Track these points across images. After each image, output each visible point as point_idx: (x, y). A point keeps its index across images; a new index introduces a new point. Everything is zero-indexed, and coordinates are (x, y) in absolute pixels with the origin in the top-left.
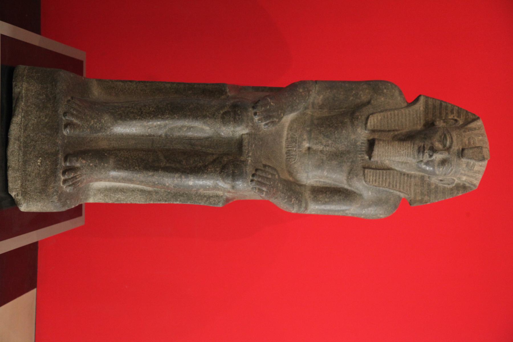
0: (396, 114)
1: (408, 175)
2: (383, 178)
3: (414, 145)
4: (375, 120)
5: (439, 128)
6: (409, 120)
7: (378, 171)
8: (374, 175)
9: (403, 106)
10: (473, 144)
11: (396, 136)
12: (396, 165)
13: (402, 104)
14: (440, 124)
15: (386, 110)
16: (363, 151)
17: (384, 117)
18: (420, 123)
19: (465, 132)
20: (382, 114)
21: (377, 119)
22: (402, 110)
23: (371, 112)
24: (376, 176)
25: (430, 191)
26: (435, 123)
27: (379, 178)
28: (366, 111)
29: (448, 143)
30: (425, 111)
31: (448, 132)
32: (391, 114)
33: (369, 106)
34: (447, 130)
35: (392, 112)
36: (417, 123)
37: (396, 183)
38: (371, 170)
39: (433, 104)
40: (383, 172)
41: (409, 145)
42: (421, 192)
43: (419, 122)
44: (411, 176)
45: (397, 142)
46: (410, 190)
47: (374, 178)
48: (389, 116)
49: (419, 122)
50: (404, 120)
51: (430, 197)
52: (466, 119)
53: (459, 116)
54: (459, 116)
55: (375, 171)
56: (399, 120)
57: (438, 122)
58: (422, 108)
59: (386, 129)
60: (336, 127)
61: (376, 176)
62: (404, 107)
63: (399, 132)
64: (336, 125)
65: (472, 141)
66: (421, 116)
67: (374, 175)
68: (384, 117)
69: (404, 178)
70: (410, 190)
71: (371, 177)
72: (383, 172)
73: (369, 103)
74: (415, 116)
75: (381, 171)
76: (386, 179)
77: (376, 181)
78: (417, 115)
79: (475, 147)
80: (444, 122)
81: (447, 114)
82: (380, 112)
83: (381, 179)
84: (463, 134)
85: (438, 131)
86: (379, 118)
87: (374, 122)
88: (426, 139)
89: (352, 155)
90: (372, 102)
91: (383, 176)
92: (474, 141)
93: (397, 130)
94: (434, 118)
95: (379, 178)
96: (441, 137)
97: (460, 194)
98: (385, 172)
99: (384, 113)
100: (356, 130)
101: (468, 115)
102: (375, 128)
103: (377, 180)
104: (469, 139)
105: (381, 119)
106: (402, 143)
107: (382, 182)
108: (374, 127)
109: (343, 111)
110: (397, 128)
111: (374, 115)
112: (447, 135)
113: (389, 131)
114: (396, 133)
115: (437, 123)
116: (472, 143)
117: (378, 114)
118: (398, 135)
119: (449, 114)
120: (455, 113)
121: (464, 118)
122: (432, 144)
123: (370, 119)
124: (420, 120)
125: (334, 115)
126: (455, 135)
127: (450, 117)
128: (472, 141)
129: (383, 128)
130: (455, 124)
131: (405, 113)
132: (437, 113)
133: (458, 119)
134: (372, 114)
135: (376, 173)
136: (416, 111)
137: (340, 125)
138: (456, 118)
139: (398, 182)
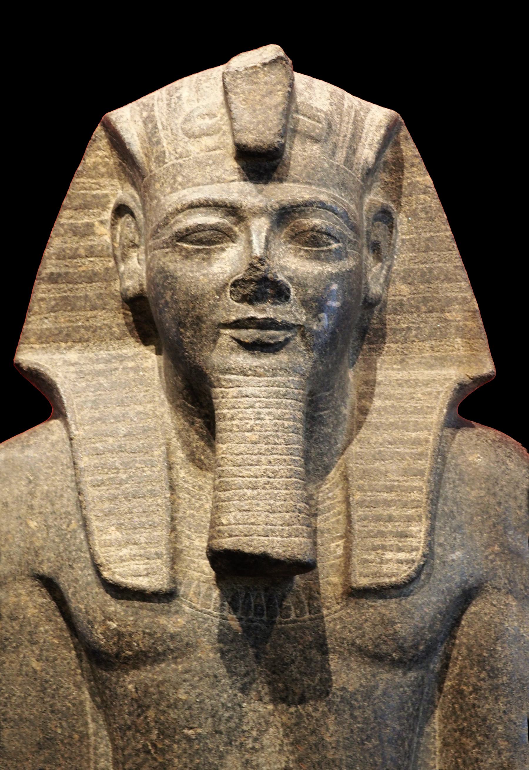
0: (96, 461)
1: (362, 396)
2: (388, 504)
3: (228, 371)
4: (125, 552)
5: (149, 269)
6: (121, 403)
7: (357, 527)
8: (378, 542)
9: (64, 434)
10: (211, 115)
11: (192, 457)
12: (324, 448)
13: (54, 438)
14: (135, 272)
15: (80, 505)
16: (270, 600)
17: (109, 513)
18: (133, 358)
19: (160, 159)
20: (94, 524)
21: (120, 545)
22: (77, 433)
23: (89, 575)
24: (382, 534)
25: (425, 300)
26: (130, 294)
27: (390, 519)
28: (88, 598)
29: (213, 219)
30: (80, 341)
31: (166, 223)
32: (97, 485)
33: (63, 581)
34: (155, 234)
35: (87, 478)
36: (136, 370)
37: (403, 442)
38: (355, 560)
39: (53, 310)
40: (361, 504)
41: (233, 392)
42: (430, 337)
43: (131, 364)
44: (366, 383)
45: (222, 447)
46: (427, 384)
47: (391, 541)
48: (103, 491)
49: (131, 364)
50: (123, 429)
51: (450, 301)
52: (111, 176)
53: (100, 203)
54: (100, 203)
55: (356, 540)
56: (121, 449)
57: (128, 283)
58: (73, 356)
59: (162, 499)
60: (161, 733)
61: (382, 534)
62: (67, 425)
63: (176, 443)
64: (154, 736)
65: (199, 122)
66: (103, 354)
67: (378, 542)
68: (109, 513)
69: (378, 411)
70: (427, 384)
71: (389, 555)
72: (361, 504)
73: (49, 585)
74: (102, 380)
75: (358, 513)
76: (390, 489)
77: (404, 535)
78: (99, 373)
79: (227, 103)
80: (125, 257)
81: (91, 252)
82: (88, 535)
83: (394, 511)
84: (170, 160)
85: (162, 270)
86: (114, 534)
87: (133, 558)
88: (199, 320)
89: (291, 651)
90: (45, 569)
91: (376, 503)
92: (202, 116)
93: (169, 453)
94: (115, 304)
95: (390, 519)
96: (188, 256)
97: (428, 180)
98: (357, 496)
99: (91, 516)
100: (172, 637)
101: (95, 166)
102: (162, 549)
103: (401, 527)
104: (192, 136)
105: (120, 527)
106: (220, 425)
107: (405, 505)
108: (159, 555)
109: (92, 695)
110: (158, 452)
111: (101, 560)
112: (176, 228)
113: (172, 488)
114: (180, 455)
115: (131, 285)
116: (208, 121)
117: (97, 538)
118: (186, 444)
119: (95, 241)
120: (86, 220)
121: (104, 181)
122: (220, 291)
123: (118, 578)
124: (122, 359)
125: (113, 740)
126: (175, 197)
127: (107, 238)
128: (199, 122)
129: (162, 517)
130: (132, 215)
131: (94, 421)
132: (91, 290)
133: (111, 206)
134: (97, 568)
135: (370, 535)
136: (81, 375)
137: (151, 713)
138: (108, 215)
139: (396, 434)
